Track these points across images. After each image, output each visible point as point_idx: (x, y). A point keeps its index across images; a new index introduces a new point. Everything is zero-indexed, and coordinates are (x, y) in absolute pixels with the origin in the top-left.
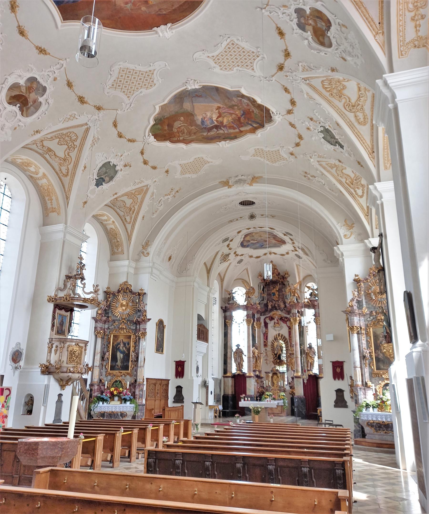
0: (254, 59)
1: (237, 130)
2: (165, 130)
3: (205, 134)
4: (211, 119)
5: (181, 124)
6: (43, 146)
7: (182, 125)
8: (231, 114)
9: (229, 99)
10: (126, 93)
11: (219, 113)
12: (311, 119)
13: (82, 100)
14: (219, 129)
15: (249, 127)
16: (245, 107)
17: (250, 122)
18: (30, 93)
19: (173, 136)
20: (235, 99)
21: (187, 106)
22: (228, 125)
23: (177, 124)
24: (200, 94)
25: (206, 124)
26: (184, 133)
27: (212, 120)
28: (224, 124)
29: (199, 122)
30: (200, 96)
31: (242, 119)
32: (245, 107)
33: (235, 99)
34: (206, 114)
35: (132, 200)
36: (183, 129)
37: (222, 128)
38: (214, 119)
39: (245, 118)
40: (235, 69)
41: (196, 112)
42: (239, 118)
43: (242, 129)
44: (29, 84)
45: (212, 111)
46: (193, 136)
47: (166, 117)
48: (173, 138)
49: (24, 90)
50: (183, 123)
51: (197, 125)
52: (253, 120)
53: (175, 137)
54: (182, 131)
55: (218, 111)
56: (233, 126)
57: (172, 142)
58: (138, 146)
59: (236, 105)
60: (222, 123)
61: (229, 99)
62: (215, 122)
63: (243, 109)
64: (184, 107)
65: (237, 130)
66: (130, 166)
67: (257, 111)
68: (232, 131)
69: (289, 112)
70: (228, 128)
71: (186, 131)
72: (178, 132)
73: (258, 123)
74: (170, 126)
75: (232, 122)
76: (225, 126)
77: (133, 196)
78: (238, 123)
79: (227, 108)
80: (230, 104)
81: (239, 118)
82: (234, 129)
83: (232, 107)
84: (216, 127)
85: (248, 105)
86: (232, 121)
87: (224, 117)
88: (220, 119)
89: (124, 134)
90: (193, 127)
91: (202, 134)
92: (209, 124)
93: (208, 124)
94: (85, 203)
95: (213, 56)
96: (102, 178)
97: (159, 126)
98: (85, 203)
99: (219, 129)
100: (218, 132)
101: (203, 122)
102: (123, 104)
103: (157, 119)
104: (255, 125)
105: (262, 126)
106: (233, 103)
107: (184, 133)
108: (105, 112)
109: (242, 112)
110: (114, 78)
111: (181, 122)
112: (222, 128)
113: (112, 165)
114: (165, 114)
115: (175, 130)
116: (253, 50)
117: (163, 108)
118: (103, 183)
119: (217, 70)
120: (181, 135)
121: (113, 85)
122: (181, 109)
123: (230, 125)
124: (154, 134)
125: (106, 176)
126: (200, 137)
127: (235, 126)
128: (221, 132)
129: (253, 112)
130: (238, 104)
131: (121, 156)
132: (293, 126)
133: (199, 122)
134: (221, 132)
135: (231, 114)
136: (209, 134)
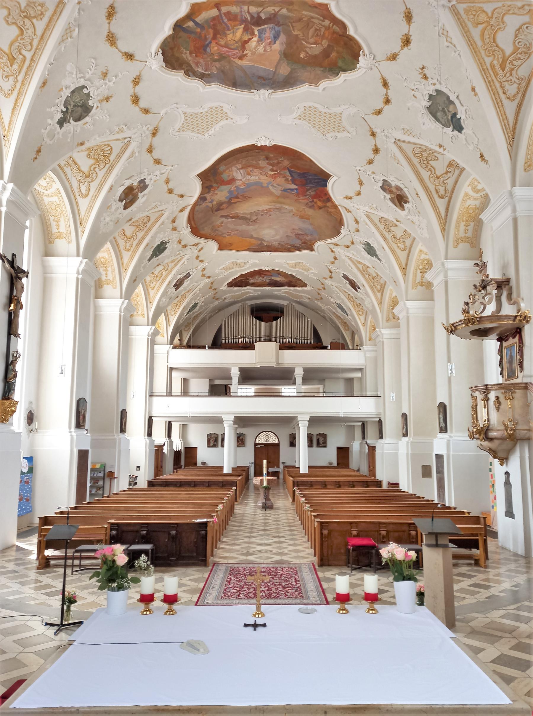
0: (183, 124)
1: (224, 9)
2: (338, 52)
3: (284, 11)
4: (260, 40)
5: (310, 48)
6: (448, 172)
7: (309, 46)
8: (226, 46)
9: (223, 72)
10: (340, 118)
11: (243, 48)
12: (107, 99)
13: (376, 151)
14: (256, 16)
15: (201, 18)
16: (201, 60)
17: (199, 30)
18: (392, 191)
19: (335, 35)
20: (214, 71)
21: (284, 70)
22: (237, 22)
23: (316, 50)
24: (259, 80)
25: (273, 32)
26: (316, 30)
27: (259, 37)
28: (243, 26)
29: (283, 38)
30: (260, 77)
31: (210, 36)
32: (201, 60)
33: (214, 71)
34: (265, 51)
35: (506, 18)
36: (312, 37)
37: (249, 18)
38: (255, 39)
39: (206, 39)
40: (206, 110)
41: (277, 57)
42: (214, 38)
43: (214, 12)
44: (388, 191)
45: (253, 54)
46: (306, 16)
47: (322, 69)
48: (337, 33)
49: (393, 196)
50: (307, 47)
51: (288, 34)
52: (193, 36)
53: (334, 32)
54: (317, 35)
55: (245, 52)
56: (229, 20)
57: (344, 26)
58: (389, 70)
59: (215, 61)
60: (246, 30)
61: (223, 72)
62: (256, 32)
63: (205, 56)
64: (289, 69)
65: (224, 9)
66: (423, 68)
67: (184, 55)
68: (234, 9)
69: (137, 81)
70: (239, 17)
71: (311, 31)
72: (323, 37)
73: (187, 31)
74: (326, 53)
75: (229, 30)
76: (243, 21)
77: (493, 22)
78: (219, 27)
79: (229, 56)
80: (223, 62)
81: (214, 38)
82: (228, 13)
83: (222, 57)
84: (258, 21)
85: (197, 64)
86: (228, 32)
87: (240, 40)
88: (246, 38)
89: (382, 99)
90: (296, 33)
91: (290, 14)
92: (268, 30)
93: (268, 30)
94: (482, 156)
95: (227, 119)
96: (452, 117)
97: (340, 63)
98: (482, 156)
99: (256, 16)
100: (260, 9)
101: (276, 37)
102: (351, 114)
103: (334, 73)
104: (191, 24)
105: (178, 26)
106: (218, 65)
107: (316, 30)
108: (373, 127)
109: (208, 50)
110: (337, 134)
111: (308, 50)
112: (249, 18)
113: (430, 103)
114: (319, 72)
115: (325, 43)
116: (184, 133)
117: (315, 81)
118: (458, 116)
119: (226, 108)
120: (323, 30)
121: (344, 130)
122: (295, 69)
123: (233, 24)
124: (355, 61)
125: (449, 111)
126: (296, 7)
127: (226, 20)
128: (253, 10)
129: (191, 53)
130: (211, 63)
131: (413, 90)
132: (130, 56)
133: (283, 38)
134: (253, 10)
135: (226, 46)
136: (277, 9)
